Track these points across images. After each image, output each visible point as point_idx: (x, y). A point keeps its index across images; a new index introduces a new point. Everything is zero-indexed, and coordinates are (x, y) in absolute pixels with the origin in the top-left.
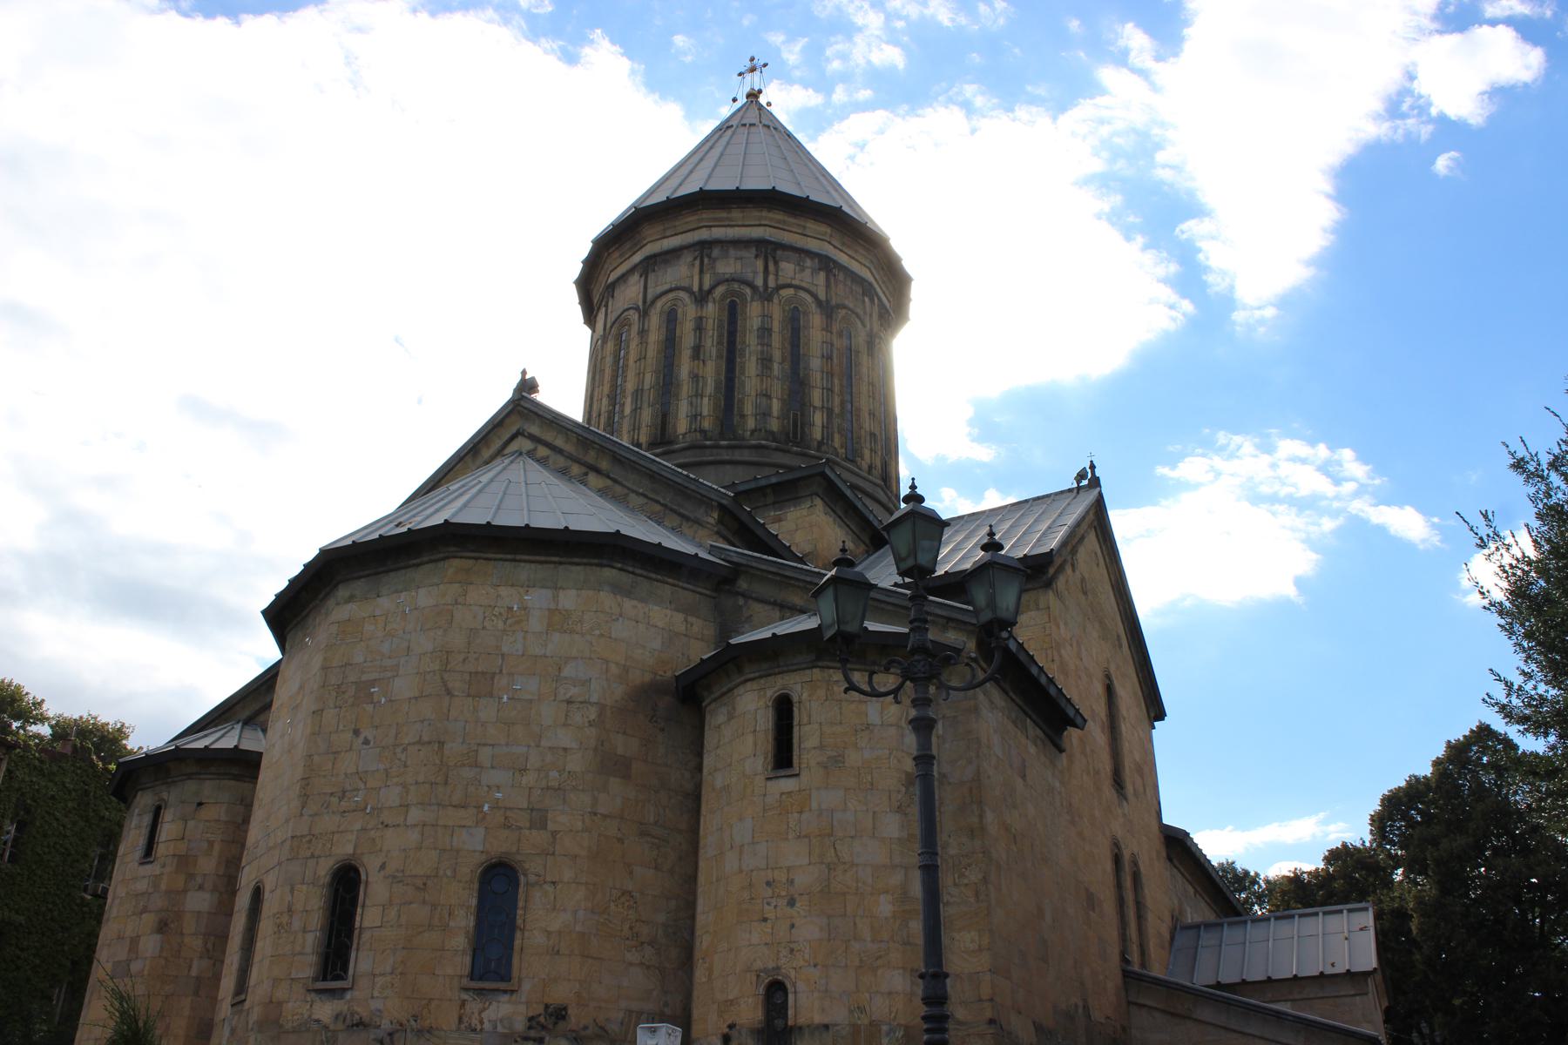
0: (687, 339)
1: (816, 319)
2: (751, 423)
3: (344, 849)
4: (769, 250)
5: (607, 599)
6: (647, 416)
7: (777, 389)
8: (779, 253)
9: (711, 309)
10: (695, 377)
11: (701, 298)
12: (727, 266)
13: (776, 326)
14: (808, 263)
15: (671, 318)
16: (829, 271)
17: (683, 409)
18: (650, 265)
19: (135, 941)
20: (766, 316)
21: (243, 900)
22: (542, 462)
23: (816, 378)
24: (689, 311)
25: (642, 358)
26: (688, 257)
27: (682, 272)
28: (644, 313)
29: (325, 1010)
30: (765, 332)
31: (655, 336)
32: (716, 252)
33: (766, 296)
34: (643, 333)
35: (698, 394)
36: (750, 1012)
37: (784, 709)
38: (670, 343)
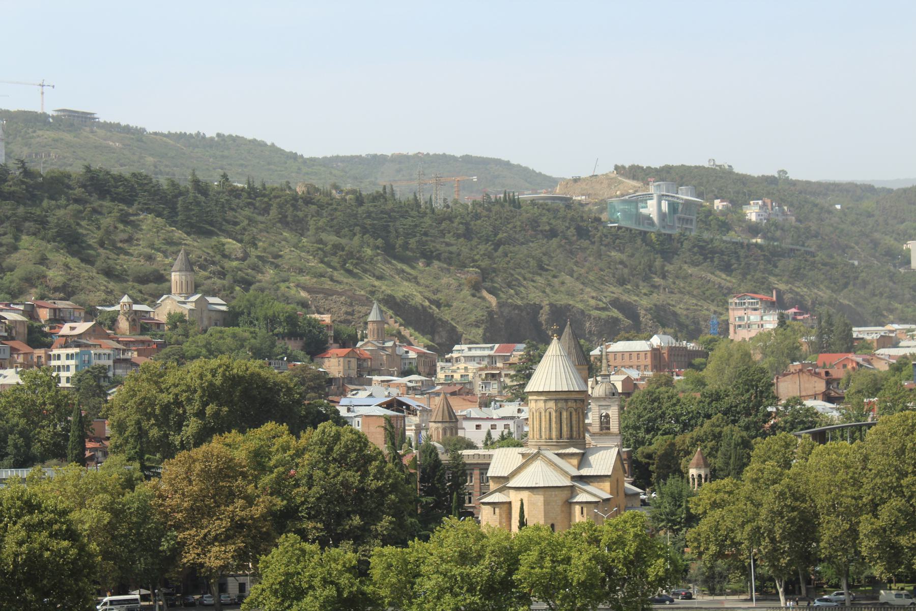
0: (554, 420)
1: (574, 413)
4: (566, 400)
7: (569, 430)
11: (556, 411)
12: (560, 405)
18: (545, 401)
25: (546, 421)
31: (548, 417)
33: (567, 410)
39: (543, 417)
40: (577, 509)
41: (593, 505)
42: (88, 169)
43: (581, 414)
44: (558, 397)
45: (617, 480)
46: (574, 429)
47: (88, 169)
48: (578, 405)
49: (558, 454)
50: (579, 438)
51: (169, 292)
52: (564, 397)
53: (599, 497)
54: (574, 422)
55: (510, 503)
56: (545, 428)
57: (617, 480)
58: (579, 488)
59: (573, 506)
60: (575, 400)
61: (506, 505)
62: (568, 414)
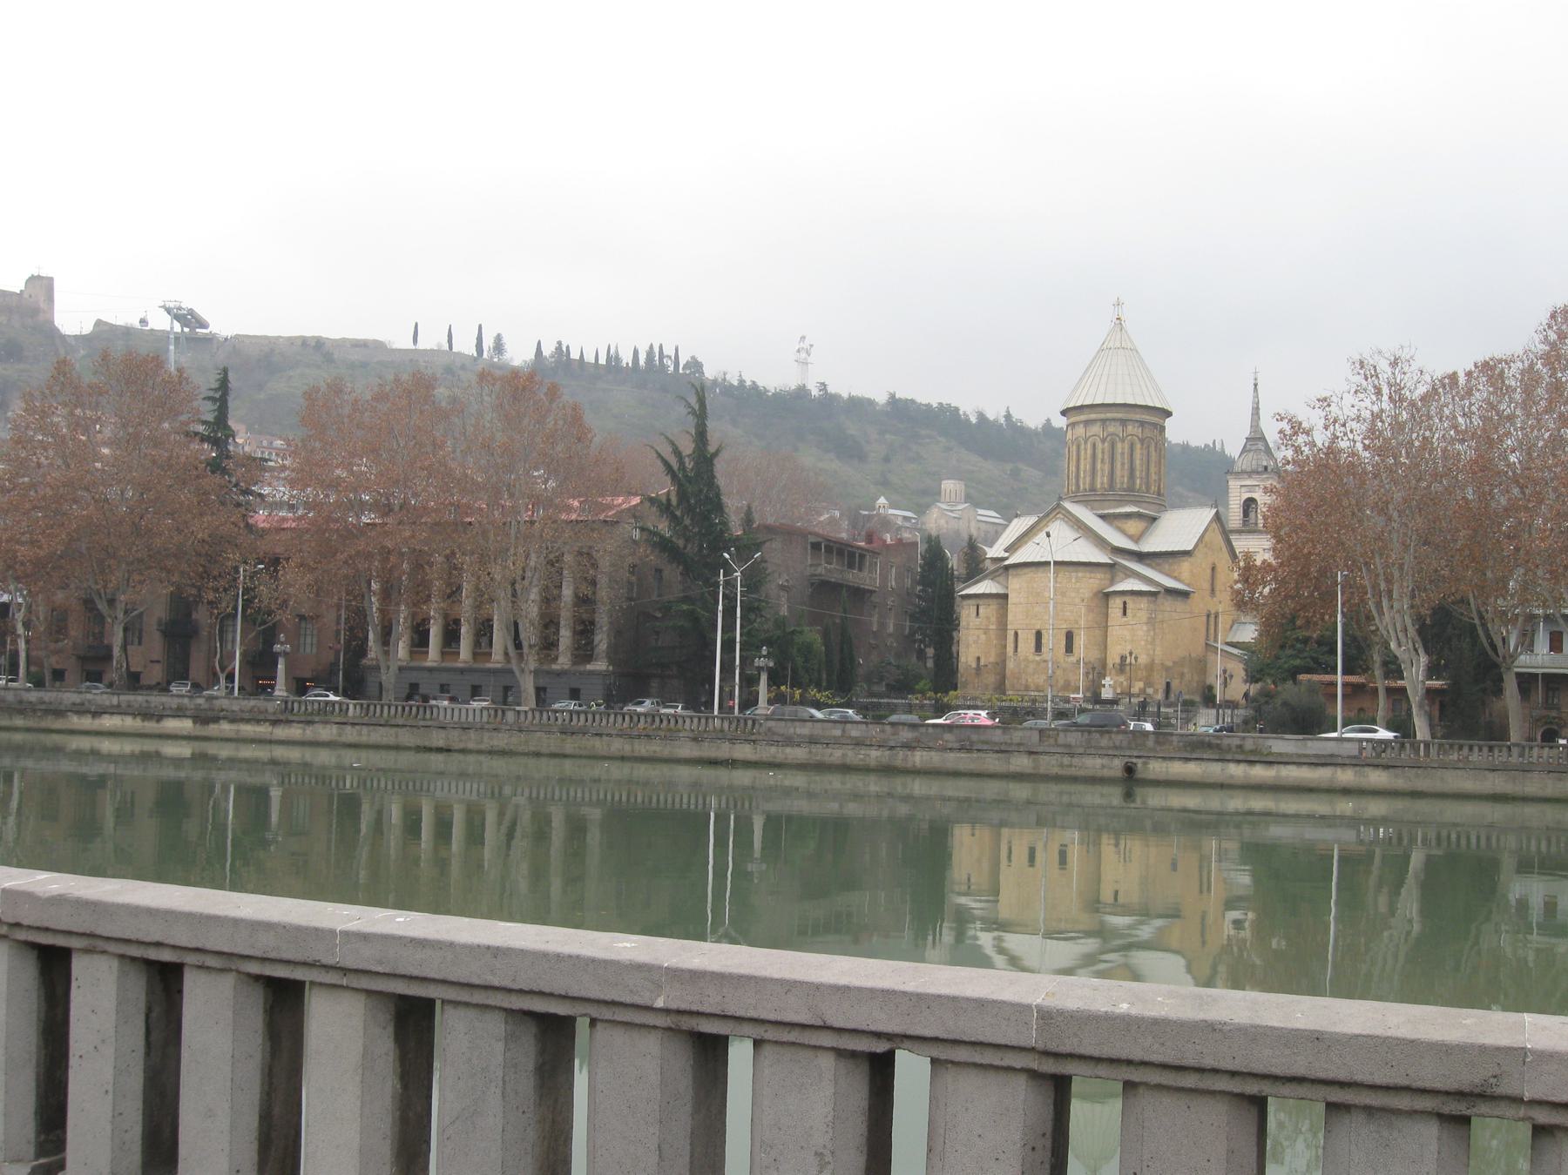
1: (1138, 446)
2: (1118, 486)
3: (1038, 627)
4: (1124, 422)
5: (1088, 575)
6: (1088, 479)
7: (1126, 473)
8: (1128, 423)
9: (1106, 444)
10: (1102, 470)
11: (1103, 441)
12: (1111, 429)
13: (1126, 451)
14: (1136, 425)
15: (1094, 446)
16: (1142, 426)
17: (1099, 480)
18: (1087, 423)
19: (978, 637)
20: (1123, 449)
21: (1010, 635)
22: (1066, 522)
23: (1138, 467)
24: (1099, 446)
25: (1085, 459)
26: (1099, 424)
27: (1096, 429)
28: (1086, 443)
29: (1038, 658)
30: (1123, 454)
31: (1089, 452)
32: (1108, 423)
33: (1123, 441)
34: (1086, 449)
35: (1103, 476)
36: (1118, 661)
37: (1125, 603)
38: (1094, 456)
39: (1083, 453)
40: (1116, 604)
41: (1145, 600)
42: (893, 396)
43: (1152, 449)
44: (1109, 415)
45: (1213, 569)
46: (1138, 474)
47: (893, 396)
48: (1148, 433)
49: (1102, 517)
50: (1148, 492)
51: (939, 502)
52: (1120, 416)
53: (1158, 584)
54: (1138, 462)
55: (1005, 597)
56: (1085, 471)
57: (1213, 569)
58: (1126, 568)
59: (1111, 602)
60: (1142, 424)
61: (1000, 601)
62: (1127, 446)
